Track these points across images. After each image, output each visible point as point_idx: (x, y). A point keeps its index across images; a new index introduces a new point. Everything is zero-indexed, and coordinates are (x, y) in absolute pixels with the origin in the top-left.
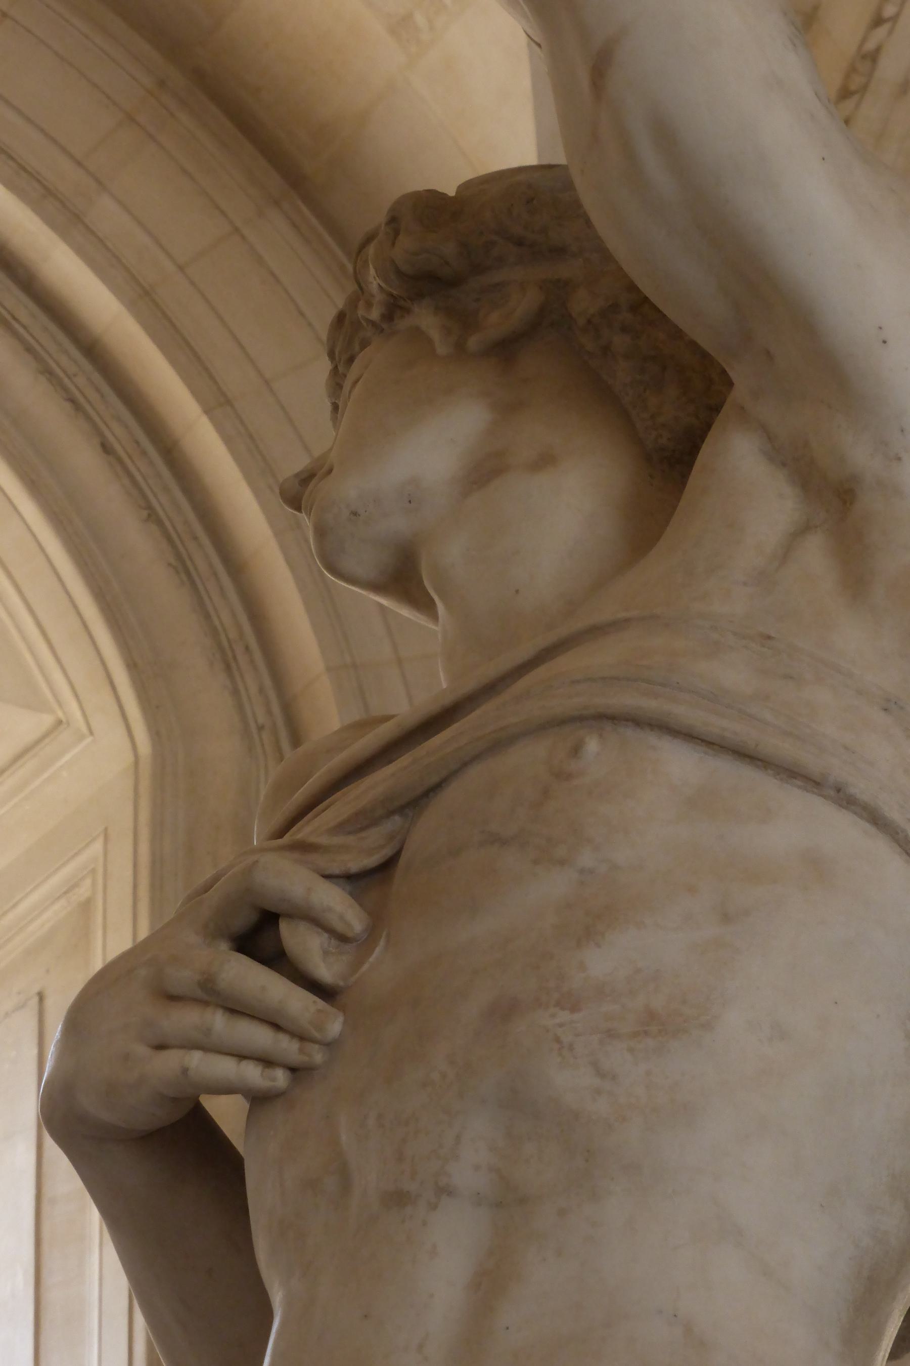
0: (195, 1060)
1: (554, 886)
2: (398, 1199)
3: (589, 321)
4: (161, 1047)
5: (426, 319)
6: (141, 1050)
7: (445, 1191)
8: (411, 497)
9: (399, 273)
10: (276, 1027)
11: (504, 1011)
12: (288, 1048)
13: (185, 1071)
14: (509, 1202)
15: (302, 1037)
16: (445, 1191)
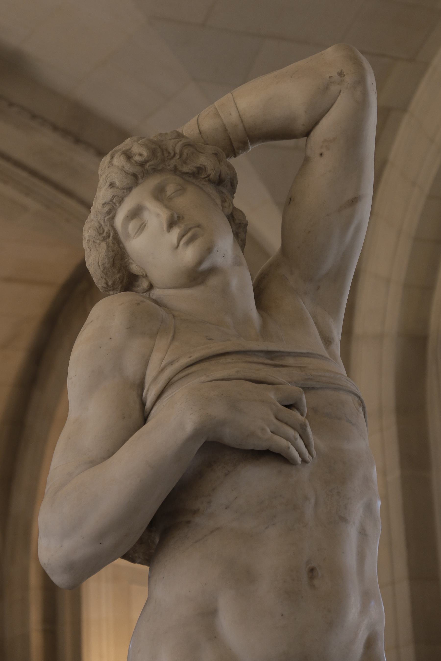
3: (240, 223)
4: (272, 432)
5: (210, 189)
10: (306, 446)
13: (289, 448)
15: (310, 453)
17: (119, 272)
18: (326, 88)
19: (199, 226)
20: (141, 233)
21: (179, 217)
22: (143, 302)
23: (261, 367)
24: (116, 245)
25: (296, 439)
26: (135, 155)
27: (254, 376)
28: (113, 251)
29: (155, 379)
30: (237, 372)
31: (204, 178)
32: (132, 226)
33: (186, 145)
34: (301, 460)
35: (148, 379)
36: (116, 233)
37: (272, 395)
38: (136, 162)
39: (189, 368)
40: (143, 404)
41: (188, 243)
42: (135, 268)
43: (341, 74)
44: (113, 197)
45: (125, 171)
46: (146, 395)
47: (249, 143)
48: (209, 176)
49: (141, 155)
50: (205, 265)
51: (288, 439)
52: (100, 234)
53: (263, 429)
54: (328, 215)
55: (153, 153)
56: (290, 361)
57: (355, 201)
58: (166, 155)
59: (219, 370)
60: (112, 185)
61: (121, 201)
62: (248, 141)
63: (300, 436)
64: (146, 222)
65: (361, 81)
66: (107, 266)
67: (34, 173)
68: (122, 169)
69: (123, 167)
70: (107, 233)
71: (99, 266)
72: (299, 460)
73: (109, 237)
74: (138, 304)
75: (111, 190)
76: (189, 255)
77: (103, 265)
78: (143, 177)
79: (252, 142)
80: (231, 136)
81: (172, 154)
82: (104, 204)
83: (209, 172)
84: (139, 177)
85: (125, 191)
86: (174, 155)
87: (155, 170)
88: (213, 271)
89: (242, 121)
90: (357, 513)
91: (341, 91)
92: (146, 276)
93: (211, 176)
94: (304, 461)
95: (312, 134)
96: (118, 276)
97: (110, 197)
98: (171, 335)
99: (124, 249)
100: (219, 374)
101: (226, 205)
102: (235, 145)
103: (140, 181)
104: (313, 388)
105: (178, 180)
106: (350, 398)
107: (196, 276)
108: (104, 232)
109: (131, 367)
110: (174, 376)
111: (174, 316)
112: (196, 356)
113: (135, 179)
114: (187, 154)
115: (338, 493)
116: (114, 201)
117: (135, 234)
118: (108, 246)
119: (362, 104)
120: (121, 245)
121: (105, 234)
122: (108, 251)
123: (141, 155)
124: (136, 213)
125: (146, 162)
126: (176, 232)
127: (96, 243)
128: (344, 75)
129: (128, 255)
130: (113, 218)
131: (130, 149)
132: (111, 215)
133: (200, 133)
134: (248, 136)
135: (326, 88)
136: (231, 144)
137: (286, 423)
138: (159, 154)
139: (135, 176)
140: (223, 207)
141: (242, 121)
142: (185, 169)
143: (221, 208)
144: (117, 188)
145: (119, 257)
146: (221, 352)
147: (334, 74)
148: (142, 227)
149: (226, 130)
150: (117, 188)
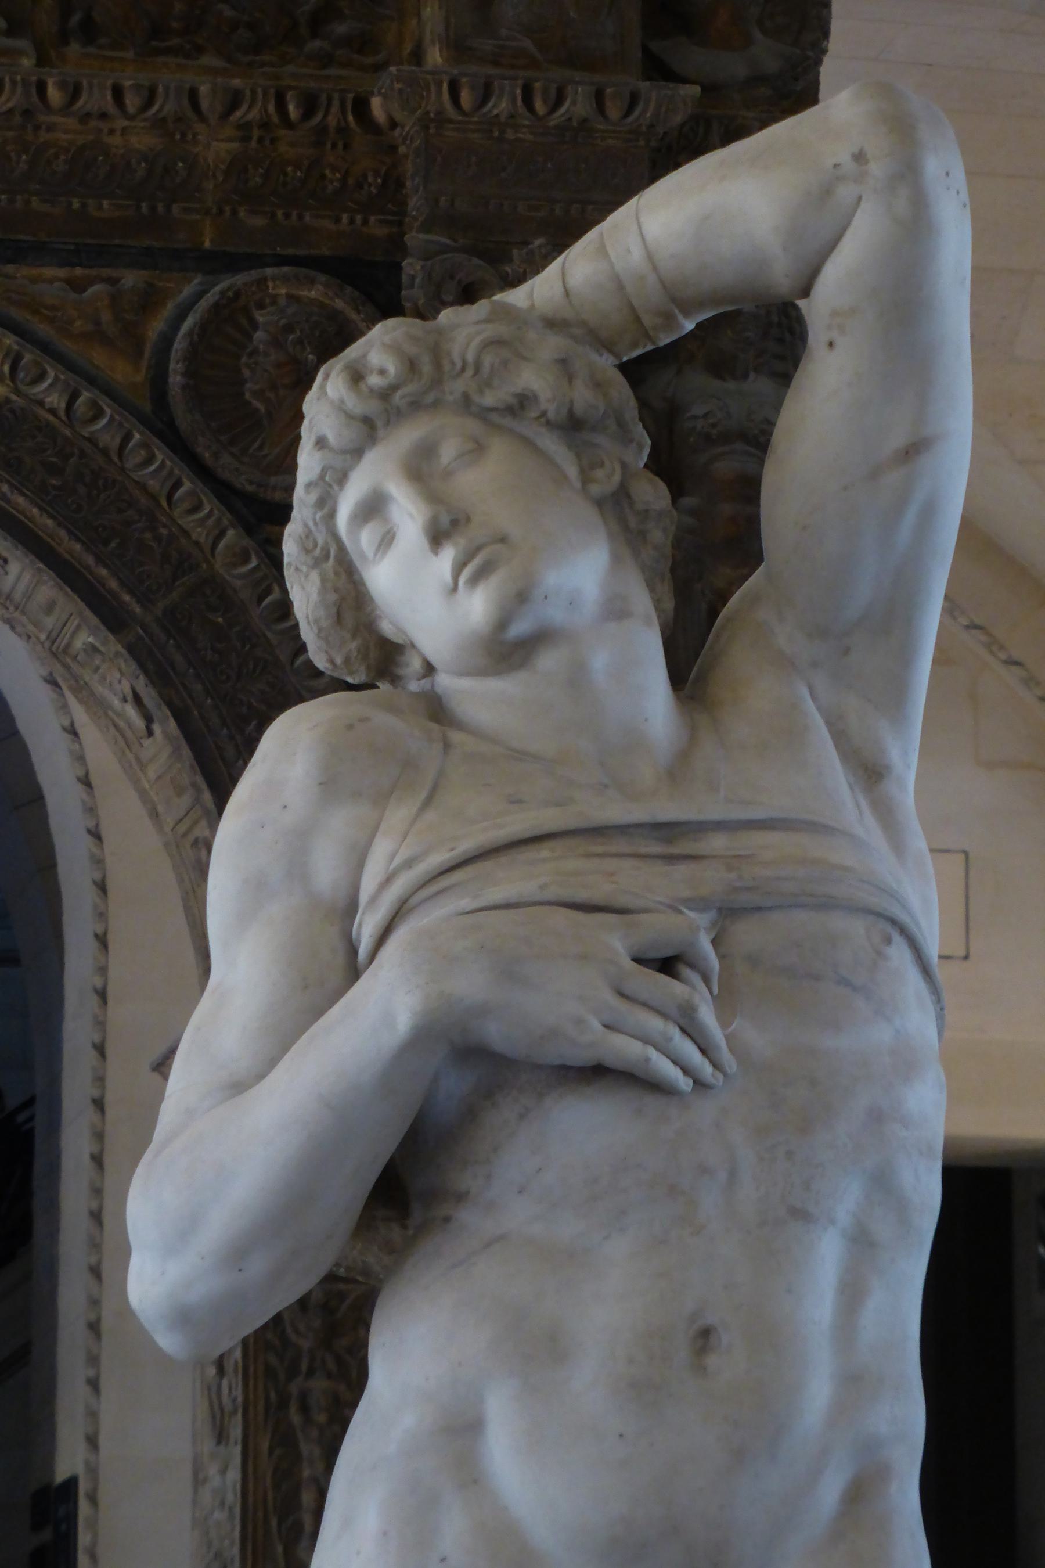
0: (653, 1054)
1: (881, 1034)
2: (801, 1215)
3: (647, 511)
4: (606, 1026)
5: (552, 444)
6: (596, 1024)
7: (832, 1222)
8: (573, 602)
9: (571, 412)
10: (703, 1051)
11: (877, 1117)
12: (706, 1069)
13: (648, 1060)
14: (862, 1243)
15: (716, 1065)
16: (832, 1222)
17: (354, 636)
18: (827, 192)
19: (503, 540)
20: (385, 553)
21: (455, 523)
22: (362, 720)
23: (627, 864)
24: (343, 576)
25: (670, 1039)
26: (372, 372)
27: (582, 895)
28: (336, 590)
29: (374, 900)
30: (542, 887)
31: (537, 418)
32: (367, 538)
33: (492, 343)
34: (691, 1082)
35: (364, 897)
36: (341, 548)
37: (616, 942)
38: (371, 390)
39: (445, 876)
40: (355, 952)
41: (475, 580)
42: (386, 628)
43: (860, 157)
44: (324, 471)
45: (345, 412)
46: (359, 934)
47: (680, 317)
48: (544, 414)
49: (382, 372)
50: (519, 628)
51: (647, 1041)
52: (308, 552)
53: (579, 1022)
54: (845, 488)
55: (412, 366)
56: (717, 843)
58: (447, 367)
59: (511, 881)
60: (321, 443)
61: (342, 478)
62: (676, 311)
63: (683, 1030)
64: (395, 529)
65: (908, 173)
66: (325, 623)
68: (340, 408)
69: (342, 401)
70: (322, 549)
71: (309, 623)
72: (684, 1083)
73: (327, 557)
74: (350, 727)
75: (318, 455)
76: (477, 607)
77: (316, 621)
78: (388, 423)
79: (687, 314)
80: (636, 303)
81: (459, 365)
82: (309, 486)
83: (544, 405)
84: (379, 424)
85: (348, 456)
86: (463, 369)
87: (416, 405)
88: (541, 638)
89: (655, 268)
90: (846, 1199)
91: (860, 198)
92: (413, 646)
93: (551, 415)
94: (699, 1084)
95: (812, 293)
96: (353, 645)
97: (317, 470)
98: (423, 795)
99: (364, 584)
100: (496, 894)
101: (599, 473)
102: (647, 320)
103: (381, 433)
104: (759, 909)
105: (473, 425)
106: (857, 928)
107: (506, 650)
108: (316, 546)
109: (326, 870)
110: (414, 893)
111: (447, 746)
112: (467, 846)
113: (369, 430)
114: (492, 366)
115: (789, 1154)
116: (327, 478)
117: (375, 554)
118: (324, 580)
119: (915, 230)
120: (356, 577)
121: (317, 552)
122: (323, 590)
123: (382, 372)
124: (373, 507)
125: (393, 388)
127: (301, 571)
128: (867, 162)
129: (372, 599)
130: (332, 515)
131: (365, 356)
132: (326, 510)
133: (567, 293)
134: (674, 300)
135: (827, 192)
136: (638, 319)
137: (645, 1005)
138: (426, 367)
139: (368, 422)
140: (586, 480)
141: (655, 268)
142: (489, 399)
143: (578, 485)
144: (331, 449)
145: (352, 601)
146: (528, 834)
147: (844, 156)
148: (387, 540)
149: (621, 287)
150: (331, 449)
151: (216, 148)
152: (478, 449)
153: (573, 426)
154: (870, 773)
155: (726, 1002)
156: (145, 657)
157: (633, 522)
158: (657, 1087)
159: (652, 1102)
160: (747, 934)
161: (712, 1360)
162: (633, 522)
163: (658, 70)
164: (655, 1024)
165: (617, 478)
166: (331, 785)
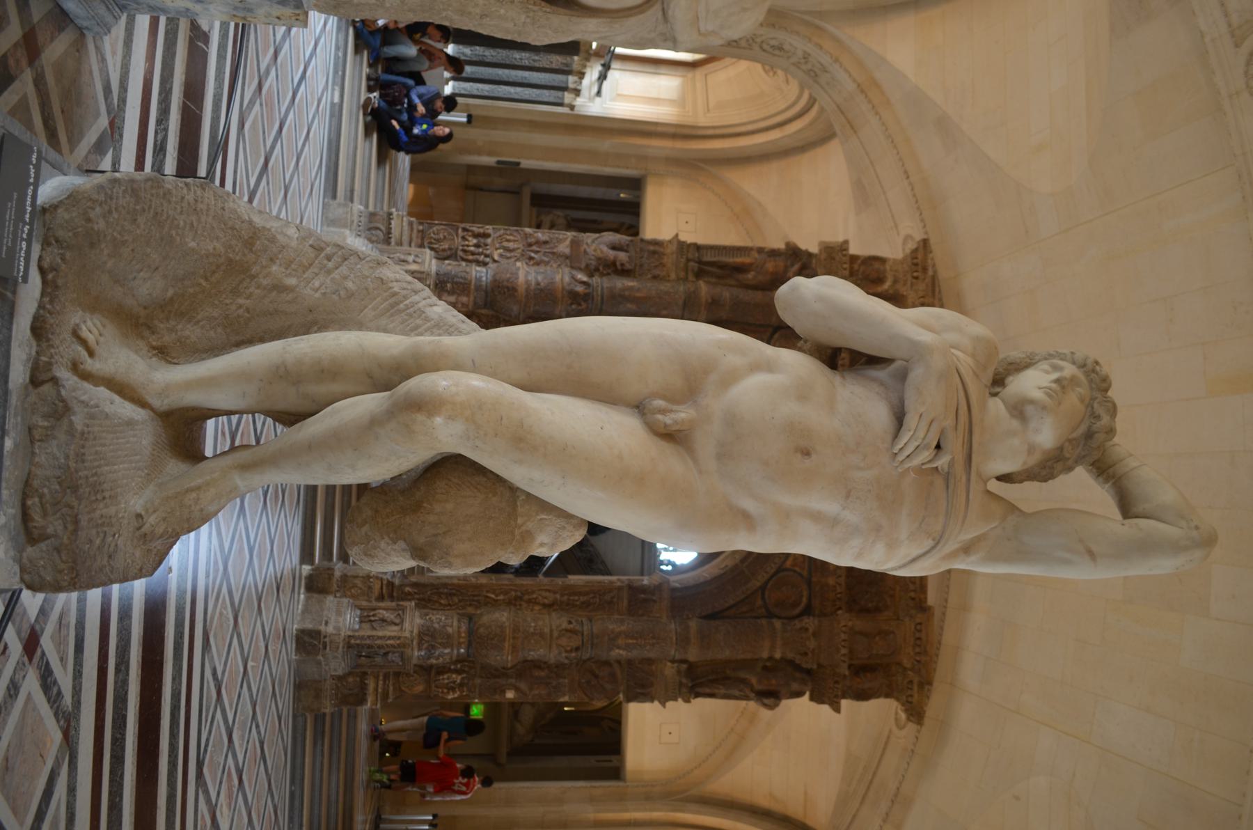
2: (848, 496)
5: (1083, 429)
6: (922, 410)
11: (878, 529)
12: (900, 458)
14: (834, 522)
41: (1047, 394)
42: (1010, 378)
50: (1029, 410)
57: (1091, 555)
67: (871, 782)
76: (1038, 395)
79: (1114, 483)
87: (1091, 381)
90: (851, 516)
102: (1111, 470)
107: (1019, 409)
126: (1054, 385)
138: (1104, 385)
140: (1070, 441)
148: (1047, 372)
151: (831, 581)
152: (1082, 401)
153: (1089, 435)
154: (967, 549)
155: (920, 470)
156: (736, 566)
157: (1049, 464)
158: (896, 436)
159: (889, 438)
160: (939, 482)
161: (799, 455)
162: (1049, 464)
163: (850, 666)
164: (921, 434)
165: (1068, 455)
166: (977, 339)
